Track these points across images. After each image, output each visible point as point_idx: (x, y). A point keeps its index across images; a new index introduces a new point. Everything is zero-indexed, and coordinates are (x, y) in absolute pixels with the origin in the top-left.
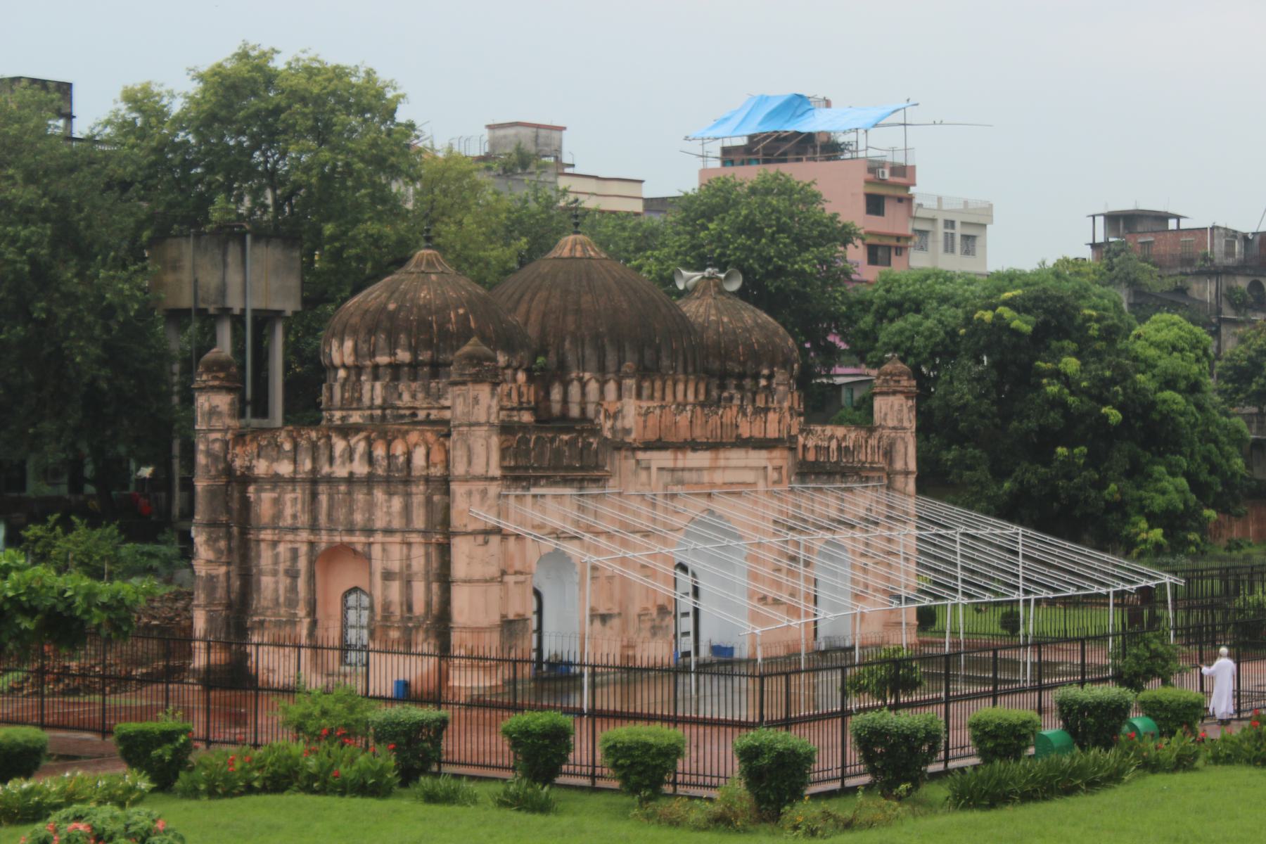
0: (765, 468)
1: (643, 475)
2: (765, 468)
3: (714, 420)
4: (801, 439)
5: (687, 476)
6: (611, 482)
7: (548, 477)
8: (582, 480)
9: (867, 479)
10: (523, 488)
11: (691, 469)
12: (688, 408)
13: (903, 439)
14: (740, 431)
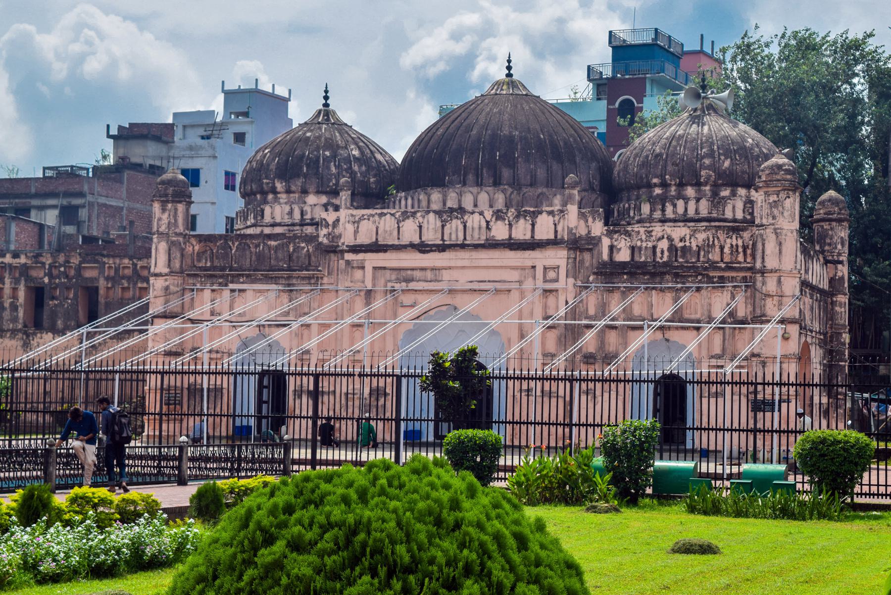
0: (534, 267)
1: (358, 274)
2: (534, 267)
3: (455, 225)
4: (606, 242)
5: (417, 274)
6: (325, 280)
7: (248, 276)
8: (289, 277)
9: (722, 279)
10: (220, 284)
11: (423, 269)
12: (419, 214)
13: (762, 235)
14: (493, 233)
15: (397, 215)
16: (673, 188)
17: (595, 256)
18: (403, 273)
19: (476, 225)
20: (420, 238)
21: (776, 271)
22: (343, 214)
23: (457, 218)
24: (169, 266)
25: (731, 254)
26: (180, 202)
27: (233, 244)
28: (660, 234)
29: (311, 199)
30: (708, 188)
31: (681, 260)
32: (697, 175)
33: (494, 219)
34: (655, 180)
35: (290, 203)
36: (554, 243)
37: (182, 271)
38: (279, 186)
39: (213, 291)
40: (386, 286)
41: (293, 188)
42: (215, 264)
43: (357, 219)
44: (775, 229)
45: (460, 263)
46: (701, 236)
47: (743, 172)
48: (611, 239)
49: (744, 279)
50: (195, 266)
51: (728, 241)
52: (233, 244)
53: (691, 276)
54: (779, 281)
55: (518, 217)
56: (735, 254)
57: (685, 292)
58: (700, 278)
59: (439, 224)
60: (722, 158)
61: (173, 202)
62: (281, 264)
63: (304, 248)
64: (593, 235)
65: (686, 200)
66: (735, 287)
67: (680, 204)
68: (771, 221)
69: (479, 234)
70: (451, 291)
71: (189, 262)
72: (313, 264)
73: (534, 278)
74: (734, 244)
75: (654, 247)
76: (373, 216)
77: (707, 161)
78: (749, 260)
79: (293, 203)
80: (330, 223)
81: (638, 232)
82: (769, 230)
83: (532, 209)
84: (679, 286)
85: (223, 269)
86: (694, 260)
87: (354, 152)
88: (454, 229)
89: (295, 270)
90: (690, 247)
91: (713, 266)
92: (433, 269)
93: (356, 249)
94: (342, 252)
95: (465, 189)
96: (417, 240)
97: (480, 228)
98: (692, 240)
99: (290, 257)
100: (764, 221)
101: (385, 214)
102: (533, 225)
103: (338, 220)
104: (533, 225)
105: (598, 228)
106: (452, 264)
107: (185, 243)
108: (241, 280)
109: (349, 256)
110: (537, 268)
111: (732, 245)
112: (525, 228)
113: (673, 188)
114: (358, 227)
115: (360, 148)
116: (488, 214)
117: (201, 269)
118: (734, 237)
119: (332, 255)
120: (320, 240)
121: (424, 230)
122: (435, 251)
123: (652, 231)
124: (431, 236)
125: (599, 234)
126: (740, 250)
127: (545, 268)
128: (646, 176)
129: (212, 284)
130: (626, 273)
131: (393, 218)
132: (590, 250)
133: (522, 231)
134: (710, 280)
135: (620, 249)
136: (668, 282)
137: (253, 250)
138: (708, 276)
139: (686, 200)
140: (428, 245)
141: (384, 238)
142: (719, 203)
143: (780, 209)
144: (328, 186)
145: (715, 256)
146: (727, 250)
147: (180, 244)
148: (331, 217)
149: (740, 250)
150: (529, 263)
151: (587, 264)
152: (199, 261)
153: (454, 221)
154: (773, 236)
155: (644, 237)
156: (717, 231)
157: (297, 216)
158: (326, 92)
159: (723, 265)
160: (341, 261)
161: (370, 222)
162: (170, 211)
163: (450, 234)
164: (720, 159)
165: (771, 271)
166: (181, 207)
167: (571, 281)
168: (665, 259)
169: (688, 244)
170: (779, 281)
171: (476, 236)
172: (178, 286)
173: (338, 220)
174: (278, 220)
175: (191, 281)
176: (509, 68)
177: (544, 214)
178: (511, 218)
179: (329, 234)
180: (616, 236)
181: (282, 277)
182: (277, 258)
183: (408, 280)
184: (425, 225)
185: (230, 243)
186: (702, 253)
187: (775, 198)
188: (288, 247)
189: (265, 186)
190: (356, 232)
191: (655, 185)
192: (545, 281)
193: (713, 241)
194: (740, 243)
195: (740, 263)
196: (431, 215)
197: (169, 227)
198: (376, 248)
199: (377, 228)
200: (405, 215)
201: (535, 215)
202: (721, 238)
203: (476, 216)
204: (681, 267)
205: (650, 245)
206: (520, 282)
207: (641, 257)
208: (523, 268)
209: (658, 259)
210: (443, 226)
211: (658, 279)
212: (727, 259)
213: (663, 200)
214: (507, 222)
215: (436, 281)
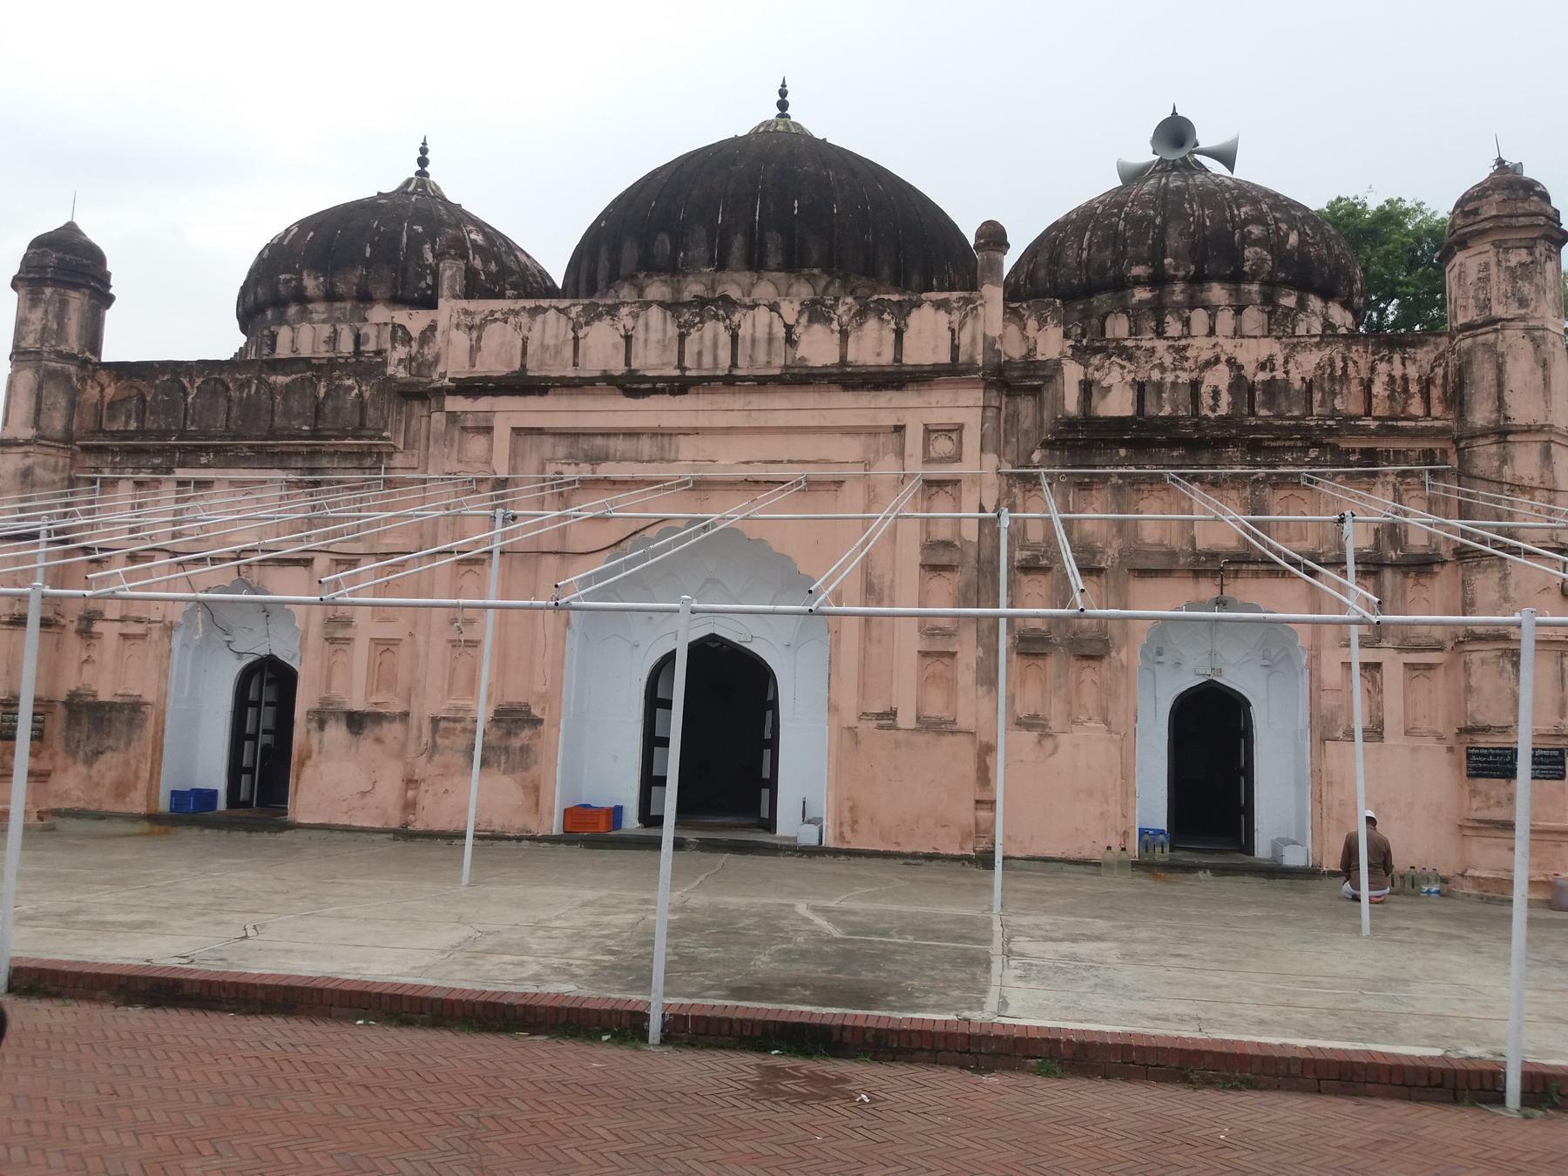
0: (899, 429)
1: (477, 444)
2: (899, 429)
4: (1073, 373)
5: (617, 445)
6: (398, 460)
7: (219, 450)
8: (314, 454)
9: (1371, 457)
10: (155, 469)
11: (632, 434)
12: (624, 311)
13: (1490, 348)
14: (802, 351)
15: (574, 312)
16: (1179, 287)
17: (1048, 405)
18: (584, 444)
19: (761, 333)
20: (628, 362)
21: (1540, 429)
22: (448, 309)
23: (716, 317)
24: (36, 423)
25: (1391, 397)
26: (76, 287)
27: (192, 382)
28: (1207, 355)
29: (379, 314)
30: (1255, 287)
31: (1263, 412)
32: (1236, 257)
33: (804, 320)
34: (1138, 270)
35: (331, 320)
36: (951, 372)
37: (68, 438)
38: (311, 284)
39: (139, 484)
40: (543, 471)
41: (341, 288)
42: (148, 425)
43: (477, 321)
44: (1528, 330)
45: (721, 421)
46: (1308, 362)
47: (1323, 263)
48: (1086, 367)
49: (1428, 457)
50: (104, 432)
51: (1382, 367)
52: (192, 382)
53: (1291, 449)
54: (1547, 455)
55: (862, 314)
56: (1400, 398)
57: (1275, 486)
58: (1313, 453)
59: (673, 331)
60: (1284, 226)
61: (56, 283)
62: (295, 424)
63: (351, 388)
64: (1039, 357)
65: (1212, 311)
66: (1403, 474)
67: (1199, 318)
68: (1514, 310)
69: (769, 353)
70: (700, 485)
71: (89, 421)
72: (369, 424)
73: (901, 453)
74: (1398, 373)
75: (1195, 385)
76: (516, 313)
77: (1256, 230)
78: (1437, 410)
79: (339, 320)
80: (415, 334)
81: (1153, 351)
82: (1513, 338)
83: (895, 298)
84: (1262, 471)
85: (164, 434)
86: (1296, 413)
87: (473, 236)
88: (708, 342)
89: (328, 438)
90: (1287, 381)
91: (1347, 424)
92: (657, 433)
93: (471, 387)
94: (442, 392)
95: (723, 276)
96: (618, 368)
97: (771, 339)
98: (1291, 366)
99: (318, 408)
100: (1498, 310)
101: (545, 310)
102: (899, 334)
103: (432, 328)
104: (899, 334)
105: (1051, 342)
106: (702, 421)
107: (82, 380)
108: (204, 460)
109: (454, 404)
110: (908, 430)
111: (1392, 377)
112: (880, 340)
113: (1179, 287)
114: (479, 338)
115: (485, 234)
116: (790, 310)
117: (113, 435)
118: (1397, 358)
119: (416, 405)
120: (390, 370)
121: (637, 347)
122: (662, 392)
123: (1185, 348)
124: (653, 359)
125: (1056, 356)
126: (1414, 388)
127: (929, 431)
128: (1114, 263)
129: (138, 469)
130: (1124, 444)
131: (563, 318)
132: (1035, 391)
133: (871, 346)
134: (1341, 458)
135: (1109, 389)
136: (1232, 464)
137: (234, 394)
138: (1335, 448)
139: (1212, 311)
140: (645, 379)
141: (541, 365)
142: (1286, 316)
143: (1538, 279)
144: (417, 289)
145: (1349, 403)
146: (1378, 389)
147: (68, 378)
148: (415, 321)
149: (1414, 388)
150: (890, 420)
151: (1026, 423)
152: (112, 419)
153: (709, 325)
154: (1528, 346)
155: (1168, 360)
156: (1348, 348)
157: (346, 345)
158: (424, 151)
159: (1373, 424)
160: (435, 416)
161: (509, 328)
162: (48, 303)
163: (700, 353)
164: (1279, 229)
165: (1528, 430)
166: (77, 301)
167: (991, 459)
168: (1223, 410)
169: (1279, 375)
170: (1547, 455)
171: (761, 357)
172: (55, 470)
173: (432, 328)
174: (305, 352)
175: (90, 462)
176: (783, 105)
177: (927, 309)
178: (845, 319)
179: (411, 359)
180: (1096, 360)
181: (297, 454)
182: (287, 413)
183: (596, 459)
184: (639, 335)
185: (185, 381)
186: (1317, 396)
187: (1523, 256)
188: (315, 387)
189: (281, 288)
190: (474, 350)
191: (1138, 282)
192: (928, 460)
193: (1345, 368)
194: (1412, 372)
195: (1415, 418)
196: (655, 313)
197: (42, 340)
198: (521, 385)
199: (525, 341)
200: (592, 315)
201: (902, 311)
202: (1362, 363)
203: (763, 315)
204: (1267, 427)
205: (1184, 377)
206: (867, 464)
207: (1161, 408)
208: (872, 432)
209: (1205, 411)
210: (682, 338)
211: (1206, 457)
212: (1380, 409)
213: (1158, 310)
214: (835, 326)
215: (662, 459)
